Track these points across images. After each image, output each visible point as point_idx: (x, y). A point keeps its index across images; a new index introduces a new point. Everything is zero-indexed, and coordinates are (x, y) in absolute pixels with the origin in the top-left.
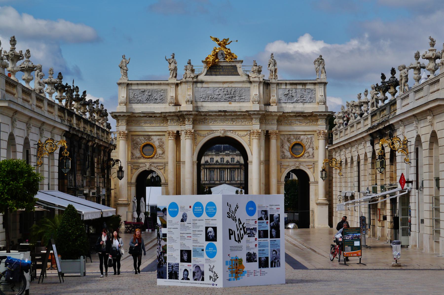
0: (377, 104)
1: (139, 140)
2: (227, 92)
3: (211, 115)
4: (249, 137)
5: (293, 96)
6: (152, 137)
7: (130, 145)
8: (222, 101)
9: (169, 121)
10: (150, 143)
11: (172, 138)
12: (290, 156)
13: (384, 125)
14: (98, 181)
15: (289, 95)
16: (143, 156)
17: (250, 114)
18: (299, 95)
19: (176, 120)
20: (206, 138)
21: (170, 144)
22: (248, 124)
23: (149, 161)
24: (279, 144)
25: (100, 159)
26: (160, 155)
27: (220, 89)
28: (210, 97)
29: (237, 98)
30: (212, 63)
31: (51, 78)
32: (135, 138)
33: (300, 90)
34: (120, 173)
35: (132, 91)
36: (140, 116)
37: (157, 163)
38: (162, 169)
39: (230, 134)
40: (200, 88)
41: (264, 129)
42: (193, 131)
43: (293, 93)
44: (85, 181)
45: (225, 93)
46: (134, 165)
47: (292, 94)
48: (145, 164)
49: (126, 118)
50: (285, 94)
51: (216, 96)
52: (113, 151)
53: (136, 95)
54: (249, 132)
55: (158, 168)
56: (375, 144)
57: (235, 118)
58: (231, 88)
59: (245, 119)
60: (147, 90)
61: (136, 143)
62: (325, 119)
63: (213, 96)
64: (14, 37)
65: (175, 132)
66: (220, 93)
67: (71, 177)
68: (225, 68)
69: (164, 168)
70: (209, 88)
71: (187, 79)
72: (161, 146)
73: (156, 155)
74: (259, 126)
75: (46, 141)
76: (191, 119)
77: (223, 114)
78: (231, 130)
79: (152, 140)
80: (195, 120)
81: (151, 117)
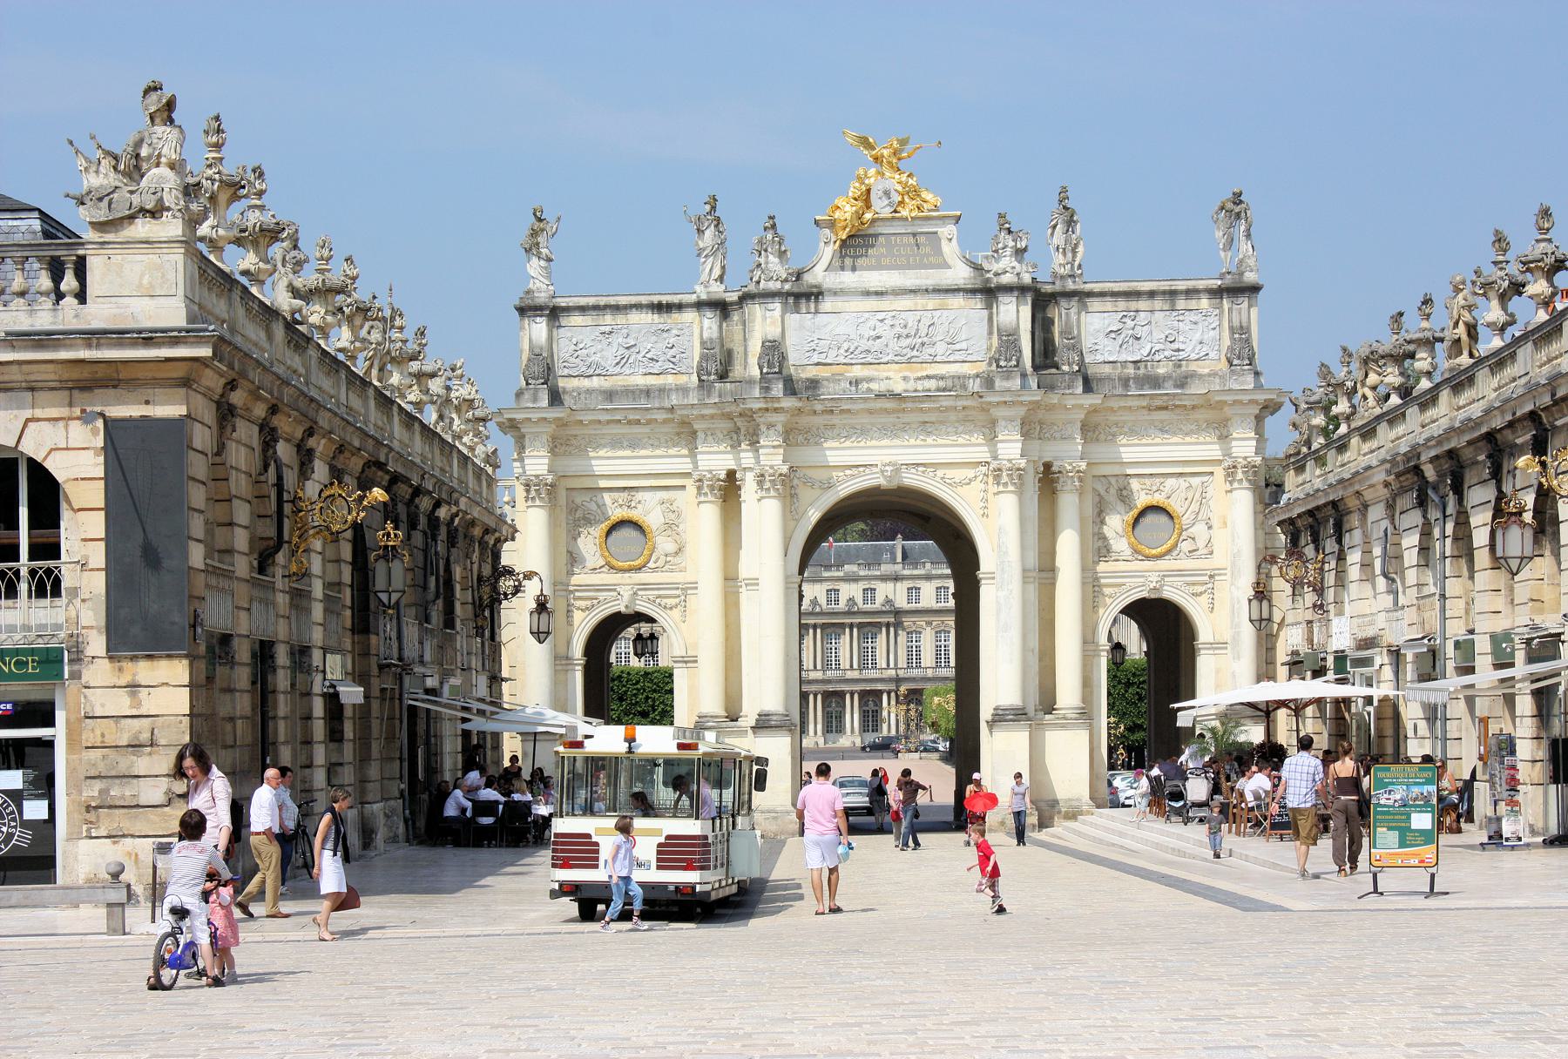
0: (1473, 343)
1: (593, 507)
2: (905, 326)
3: (849, 411)
4: (982, 486)
5: (1138, 339)
6: (640, 496)
7: (564, 525)
9: (701, 435)
10: (634, 515)
11: (710, 498)
12: (1128, 552)
13: (1514, 414)
14: (465, 646)
15: (1123, 336)
16: (608, 564)
17: (990, 403)
18: (1159, 335)
19: (725, 433)
20: (829, 494)
21: (704, 518)
22: (977, 442)
23: (628, 581)
24: (1090, 511)
25: (471, 570)
26: (668, 559)
27: (881, 316)
28: (845, 346)
29: (940, 348)
30: (853, 226)
31: (323, 274)
32: (579, 499)
33: (1162, 314)
34: (544, 616)
35: (569, 335)
36: (600, 422)
37: (658, 586)
38: (676, 606)
39: (912, 480)
41: (1036, 459)
42: (785, 469)
43: (1137, 328)
44: (429, 642)
45: (898, 329)
46: (577, 594)
47: (1133, 329)
48: (615, 590)
49: (548, 430)
50: (1111, 331)
51: (864, 345)
52: (507, 546)
53: (581, 346)
54: (984, 469)
55: (663, 604)
56: (1469, 487)
57: (933, 419)
59: (967, 424)
60: (621, 329)
61: (584, 518)
62: (1253, 418)
63: (856, 344)
64: (217, 118)
65: (723, 476)
66: (879, 331)
67: (388, 627)
68: (896, 241)
69: (683, 604)
71: (762, 285)
72: (670, 526)
73: (653, 559)
74: (1020, 445)
75: (322, 491)
77: (889, 405)
78: (918, 465)
79: (639, 506)
81: (638, 422)
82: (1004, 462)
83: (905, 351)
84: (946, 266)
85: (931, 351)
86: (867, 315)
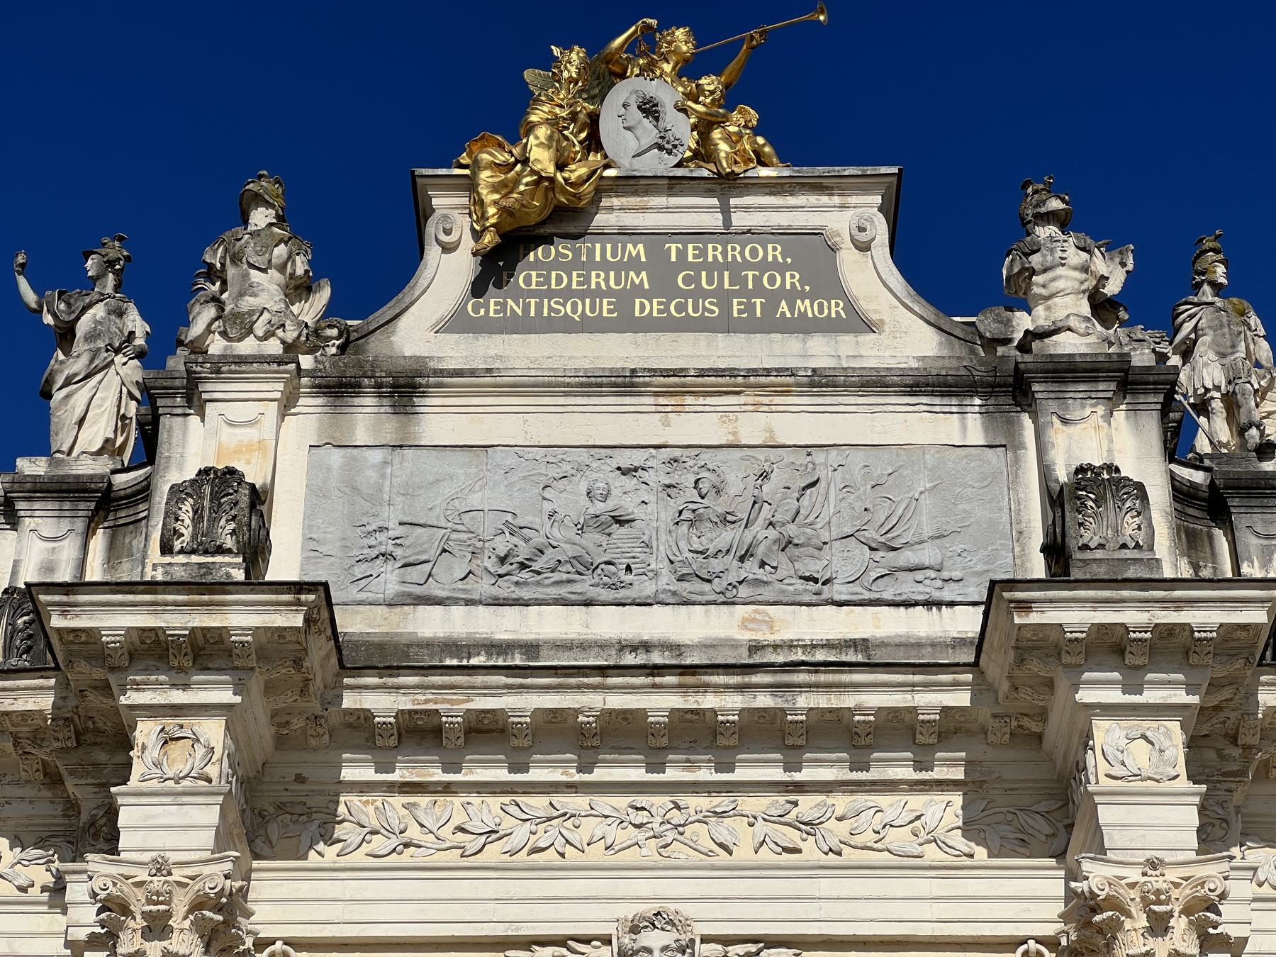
8: (647, 588)
40: (377, 456)
58: (761, 454)
63: (538, 540)
68: (682, 254)
70: (498, 454)
76: (213, 731)
80: (281, 807)
82: (1134, 875)
83: (716, 565)
84: (859, 323)
85: (813, 567)
86: (583, 456)
